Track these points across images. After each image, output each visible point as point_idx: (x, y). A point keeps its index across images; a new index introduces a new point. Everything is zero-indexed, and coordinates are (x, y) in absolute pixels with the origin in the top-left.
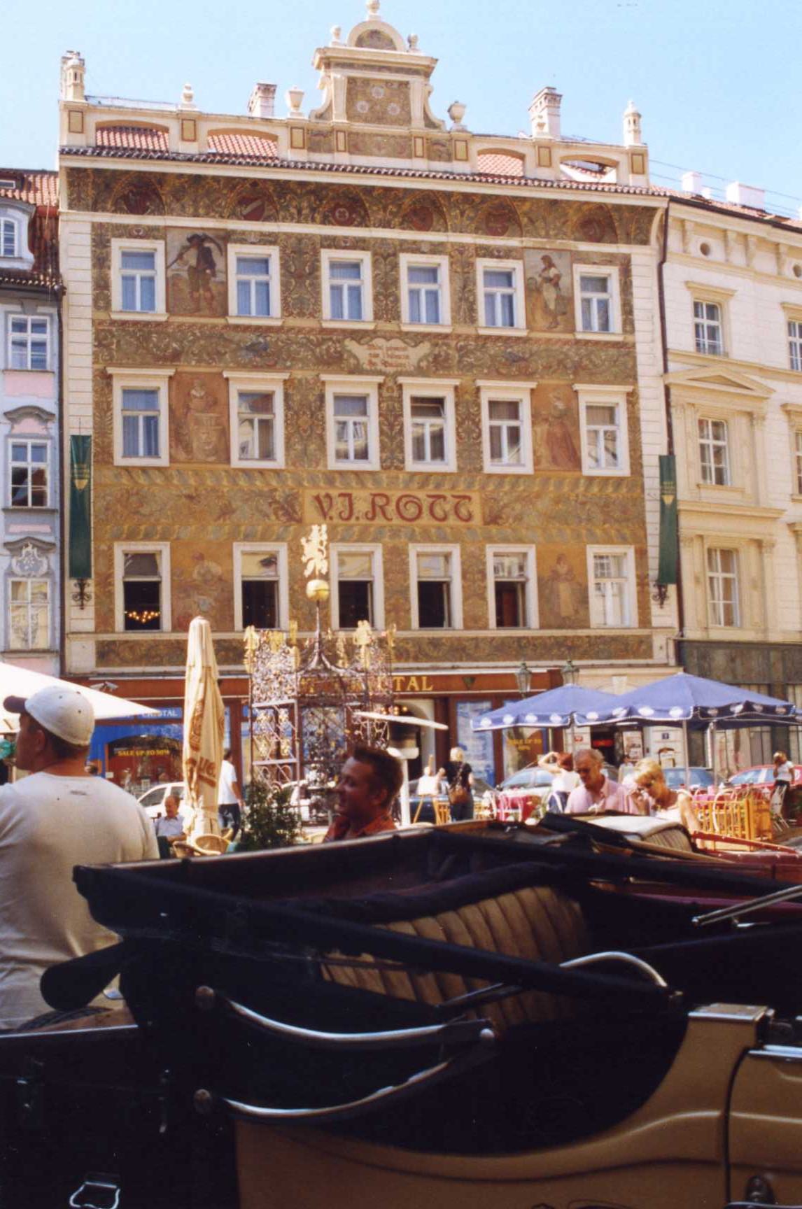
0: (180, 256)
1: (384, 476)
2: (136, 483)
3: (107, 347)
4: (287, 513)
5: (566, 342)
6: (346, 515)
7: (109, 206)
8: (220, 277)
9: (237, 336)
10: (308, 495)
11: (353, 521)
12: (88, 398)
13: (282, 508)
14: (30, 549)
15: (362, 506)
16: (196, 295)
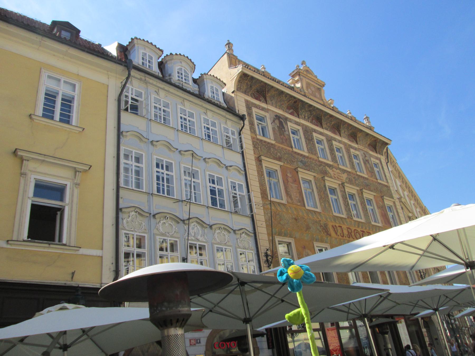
0: (274, 121)
1: (348, 220)
2: (277, 209)
3: (257, 148)
4: (326, 232)
5: (376, 182)
6: (342, 235)
7: (250, 95)
8: (287, 133)
9: (297, 156)
10: (330, 224)
11: (344, 238)
12: (255, 168)
13: (324, 229)
14: (244, 234)
15: (346, 232)
16: (281, 137)
